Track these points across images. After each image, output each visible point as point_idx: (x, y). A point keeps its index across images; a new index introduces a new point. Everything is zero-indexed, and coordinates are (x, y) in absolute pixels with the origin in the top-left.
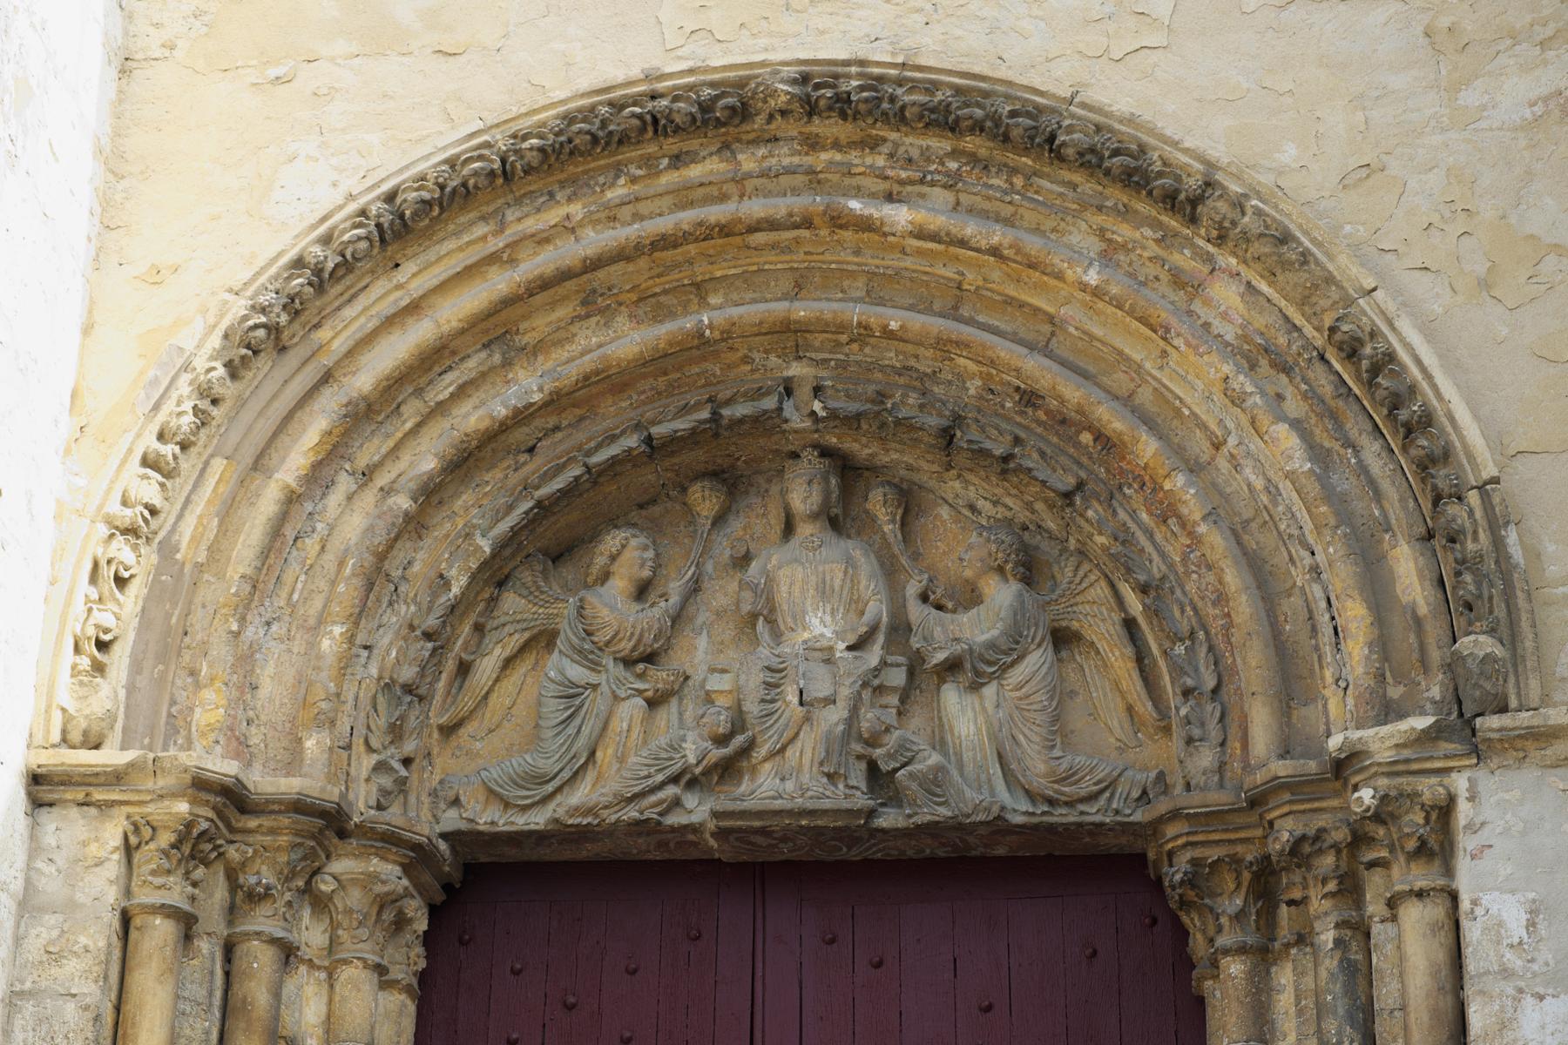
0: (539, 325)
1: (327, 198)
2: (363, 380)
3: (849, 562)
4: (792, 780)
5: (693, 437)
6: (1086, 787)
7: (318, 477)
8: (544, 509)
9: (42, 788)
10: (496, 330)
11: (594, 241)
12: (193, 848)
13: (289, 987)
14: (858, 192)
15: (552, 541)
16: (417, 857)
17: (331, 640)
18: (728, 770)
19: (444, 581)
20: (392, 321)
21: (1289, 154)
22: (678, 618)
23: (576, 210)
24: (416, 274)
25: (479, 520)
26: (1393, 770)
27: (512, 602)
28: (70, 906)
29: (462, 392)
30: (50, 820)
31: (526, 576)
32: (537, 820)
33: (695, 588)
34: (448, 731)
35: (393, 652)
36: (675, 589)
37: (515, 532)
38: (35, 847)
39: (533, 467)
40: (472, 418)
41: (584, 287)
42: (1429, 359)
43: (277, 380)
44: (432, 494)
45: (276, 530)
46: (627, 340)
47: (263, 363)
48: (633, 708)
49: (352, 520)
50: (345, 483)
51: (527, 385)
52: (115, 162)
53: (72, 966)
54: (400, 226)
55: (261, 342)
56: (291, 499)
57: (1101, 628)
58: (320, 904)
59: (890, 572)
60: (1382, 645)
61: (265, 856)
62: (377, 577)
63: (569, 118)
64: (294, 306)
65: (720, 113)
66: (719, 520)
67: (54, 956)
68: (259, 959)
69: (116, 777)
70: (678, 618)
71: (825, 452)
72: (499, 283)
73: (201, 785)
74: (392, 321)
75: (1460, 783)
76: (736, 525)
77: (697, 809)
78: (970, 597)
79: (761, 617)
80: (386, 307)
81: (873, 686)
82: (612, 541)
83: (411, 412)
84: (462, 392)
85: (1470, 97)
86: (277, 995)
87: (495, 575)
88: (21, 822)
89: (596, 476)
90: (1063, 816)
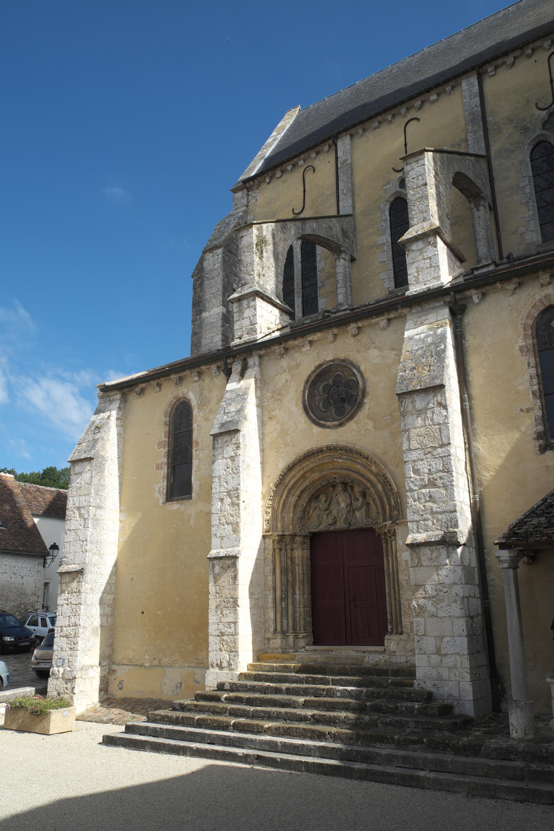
0: (308, 475)
1: (283, 465)
2: (290, 486)
3: (346, 496)
4: (341, 525)
5: (326, 484)
6: (370, 523)
7: (287, 497)
8: (312, 495)
9: (264, 537)
10: (303, 477)
11: (311, 466)
12: (279, 541)
13: (293, 552)
14: (336, 458)
15: (315, 497)
16: (305, 537)
17: (291, 514)
18: (335, 522)
19: (303, 505)
20: (292, 478)
21: (377, 451)
22: (329, 505)
23: (308, 463)
24: (293, 473)
25: (306, 497)
26: (389, 527)
27: (312, 504)
28: (268, 549)
29: (301, 484)
30: (266, 540)
31: (313, 501)
32: (316, 530)
33: (331, 499)
34: (308, 519)
35: (299, 514)
36: (328, 501)
37: (310, 498)
38: (265, 543)
39: (311, 490)
40: (302, 487)
41: (312, 470)
42: (390, 477)
43: (282, 487)
44: (299, 497)
45: (284, 504)
46: (316, 476)
47: (280, 486)
48: (325, 516)
49: (293, 499)
50: (291, 496)
51: (307, 483)
52: (263, 463)
53: (270, 555)
54: (290, 469)
55: (277, 486)
56: (285, 501)
57: (371, 502)
58: (296, 543)
59: (350, 497)
60: (390, 511)
61: (288, 539)
62: (296, 506)
63: (305, 454)
64: (281, 480)
65: (320, 451)
66: (333, 491)
67: (268, 554)
68: (289, 551)
69: (271, 535)
70: (329, 505)
71: (342, 483)
72: (302, 472)
73: (278, 536)
74: (292, 478)
75: (396, 528)
76: (336, 491)
77: (332, 528)
78: (358, 499)
79: (338, 503)
80: (291, 477)
81: (349, 511)
82: (321, 496)
83: (296, 487)
84: (301, 484)
85: (396, 441)
86: (292, 554)
87: (310, 501)
88: (263, 541)
89: (318, 490)
90: (368, 526)
